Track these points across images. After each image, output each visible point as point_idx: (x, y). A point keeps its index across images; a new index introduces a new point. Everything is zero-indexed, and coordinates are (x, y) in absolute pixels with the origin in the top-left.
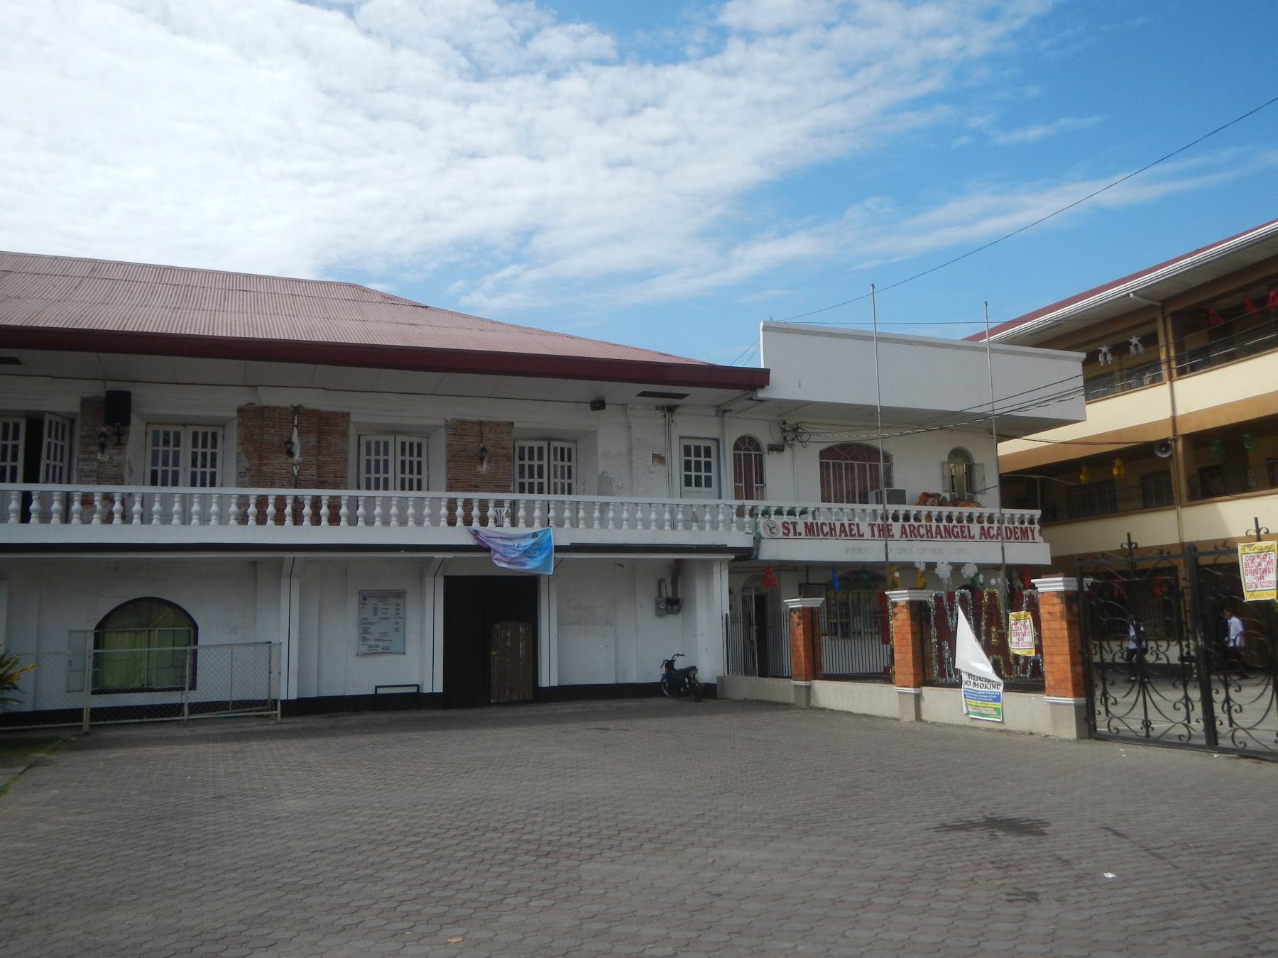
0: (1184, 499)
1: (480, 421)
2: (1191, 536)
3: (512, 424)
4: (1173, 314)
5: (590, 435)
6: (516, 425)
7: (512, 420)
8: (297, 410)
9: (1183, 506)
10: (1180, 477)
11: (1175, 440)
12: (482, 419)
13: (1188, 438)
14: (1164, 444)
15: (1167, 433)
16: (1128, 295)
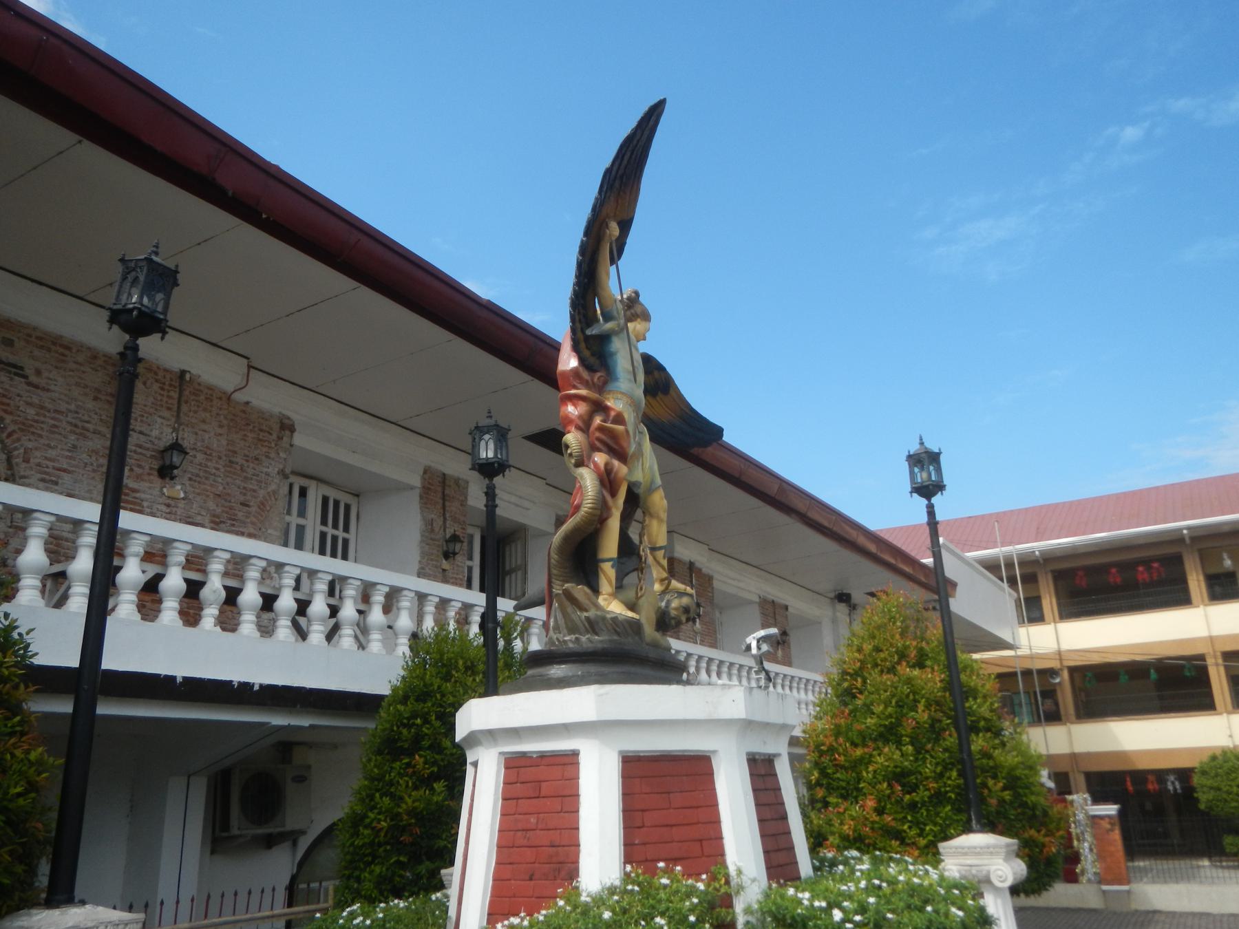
0: (1073, 718)
1: (773, 601)
2: (1079, 749)
3: (786, 608)
4: (1053, 572)
5: (811, 624)
6: (790, 609)
7: (787, 603)
8: (691, 565)
9: (1072, 723)
10: (1067, 699)
11: (1061, 669)
12: (775, 599)
13: (1073, 670)
14: (1052, 672)
15: (1054, 664)
16: (1034, 552)
